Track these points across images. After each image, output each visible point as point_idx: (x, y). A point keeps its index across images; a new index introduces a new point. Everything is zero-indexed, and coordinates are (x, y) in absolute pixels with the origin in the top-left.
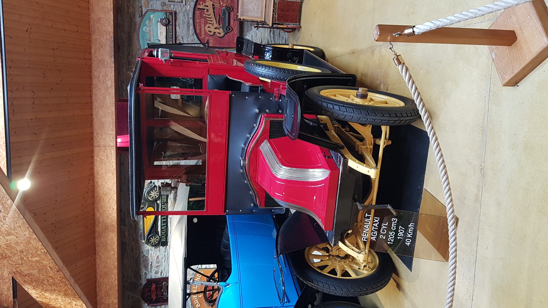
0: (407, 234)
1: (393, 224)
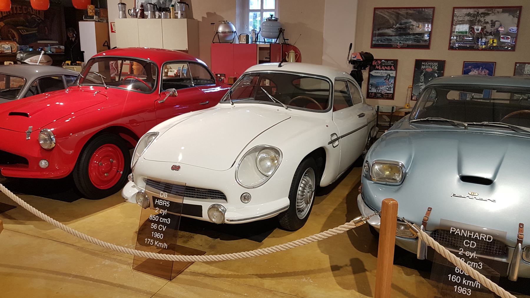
0: (158, 242)
1: (165, 220)
